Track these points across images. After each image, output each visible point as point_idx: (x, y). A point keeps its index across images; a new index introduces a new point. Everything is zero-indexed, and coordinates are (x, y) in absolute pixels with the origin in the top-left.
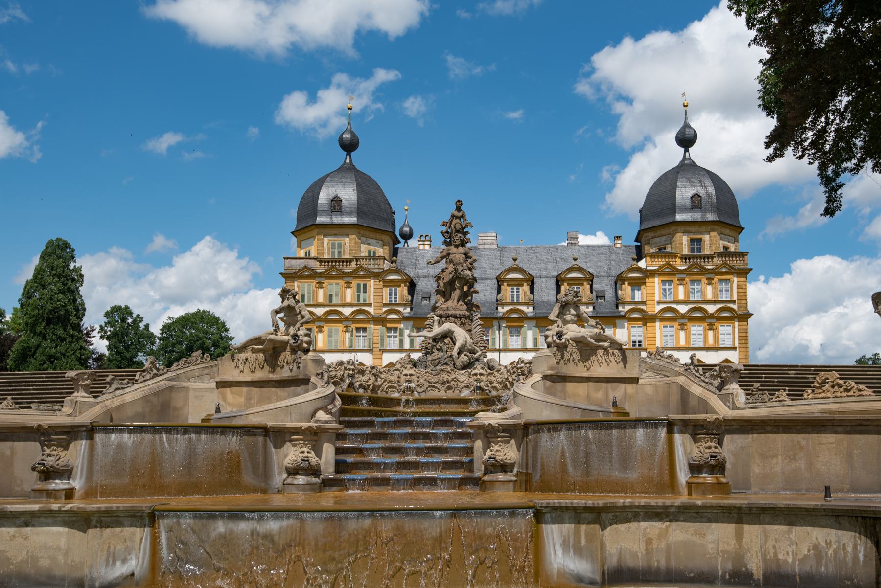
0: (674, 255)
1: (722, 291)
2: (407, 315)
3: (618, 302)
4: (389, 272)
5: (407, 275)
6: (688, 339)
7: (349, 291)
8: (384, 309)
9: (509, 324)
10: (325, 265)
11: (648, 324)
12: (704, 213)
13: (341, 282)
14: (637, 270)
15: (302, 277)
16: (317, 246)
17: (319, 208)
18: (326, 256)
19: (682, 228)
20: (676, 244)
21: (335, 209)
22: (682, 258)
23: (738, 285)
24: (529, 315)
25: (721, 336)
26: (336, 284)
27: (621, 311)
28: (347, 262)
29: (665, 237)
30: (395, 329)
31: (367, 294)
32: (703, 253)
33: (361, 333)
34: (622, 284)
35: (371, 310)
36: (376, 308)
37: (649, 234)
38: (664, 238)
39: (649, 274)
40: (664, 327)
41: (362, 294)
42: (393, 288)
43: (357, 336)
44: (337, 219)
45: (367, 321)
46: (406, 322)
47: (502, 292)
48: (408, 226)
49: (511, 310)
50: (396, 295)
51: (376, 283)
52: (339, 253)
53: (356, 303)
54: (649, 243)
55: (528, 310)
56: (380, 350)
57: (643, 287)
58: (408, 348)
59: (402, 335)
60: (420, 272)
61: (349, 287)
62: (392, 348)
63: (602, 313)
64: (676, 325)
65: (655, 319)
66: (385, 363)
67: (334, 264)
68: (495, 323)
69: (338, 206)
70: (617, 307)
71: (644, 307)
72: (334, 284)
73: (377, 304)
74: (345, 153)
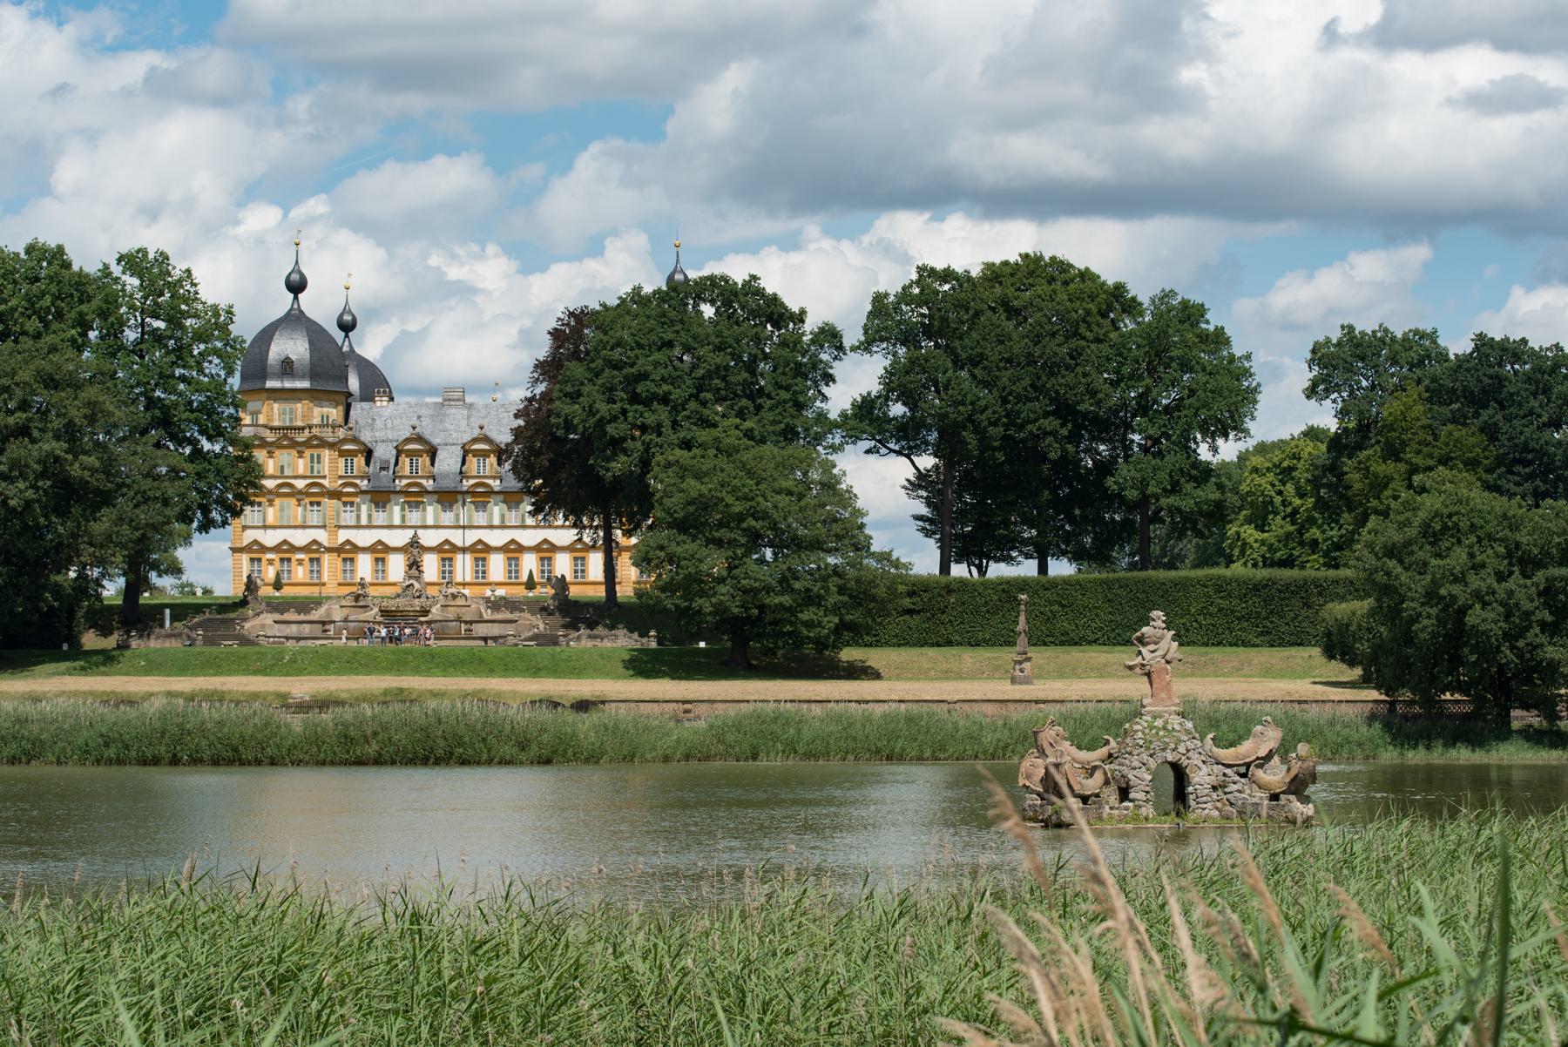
2: (364, 488)
4: (344, 441)
7: (301, 461)
8: (340, 482)
13: (294, 452)
18: (276, 423)
24: (496, 489)
33: (315, 508)
35: (325, 482)
41: (316, 465)
45: (321, 495)
46: (363, 496)
48: (350, 312)
52: (291, 419)
59: (359, 510)
60: (378, 434)
61: (301, 457)
62: (349, 523)
66: (340, 541)
68: (460, 497)
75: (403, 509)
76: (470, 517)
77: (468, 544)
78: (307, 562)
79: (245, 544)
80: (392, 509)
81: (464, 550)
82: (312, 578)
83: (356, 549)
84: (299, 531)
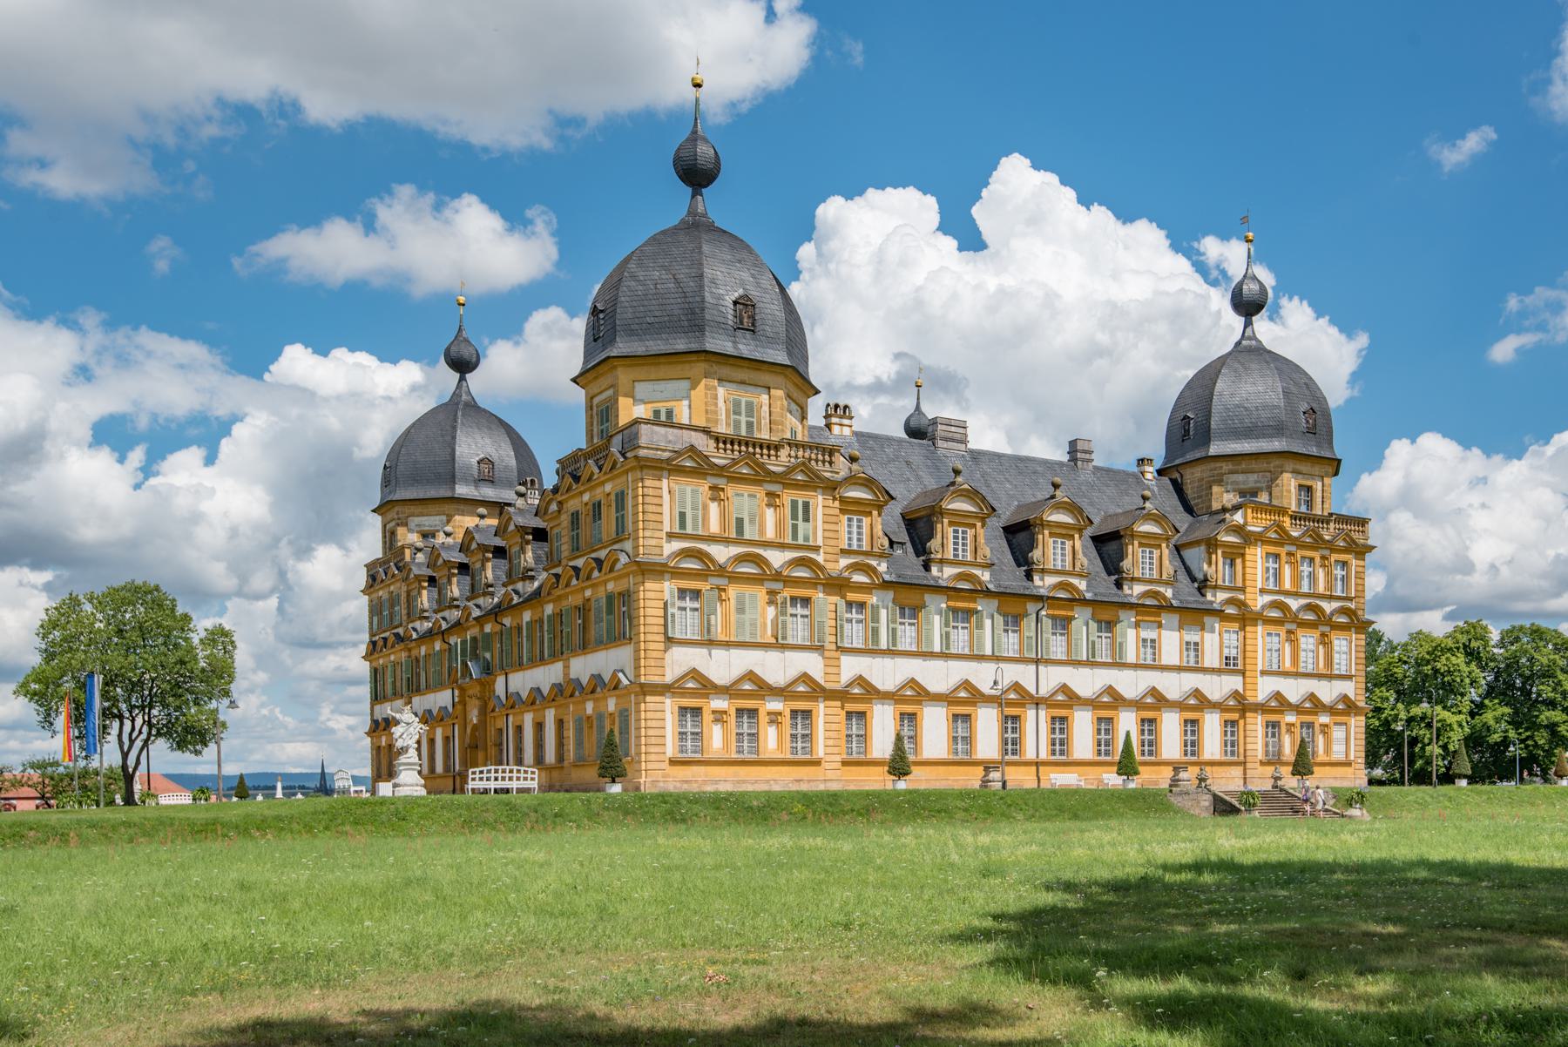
0: (1282, 511)
1: (1336, 579)
2: (887, 577)
3: (1203, 585)
4: (851, 480)
5: (887, 492)
6: (1295, 659)
7: (770, 514)
8: (844, 562)
9: (1051, 612)
10: (725, 450)
11: (1248, 629)
12: (1319, 445)
13: (760, 492)
14: (1234, 531)
15: (680, 471)
16: (706, 403)
17: (708, 317)
18: (722, 429)
19: (1289, 465)
20: (1282, 491)
21: (742, 323)
22: (1291, 516)
23: (1356, 572)
25: (1336, 656)
26: (749, 496)
27: (1212, 603)
28: (769, 448)
29: (1255, 476)
30: (861, 606)
31: (810, 525)
32: (1314, 512)
33: (799, 610)
34: (1210, 554)
35: (820, 558)
36: (828, 557)
37: (1224, 464)
38: (1253, 478)
39: (1249, 539)
40: (1269, 634)
41: (800, 523)
42: (855, 518)
43: (791, 615)
44: (746, 348)
45: (812, 583)
47: (1040, 546)
49: (1060, 583)
50: (859, 533)
51: (827, 503)
52: (750, 425)
53: (789, 540)
54: (1222, 481)
55: (1082, 585)
56: (838, 648)
57: (1239, 561)
58: (885, 648)
59: (876, 619)
62: (855, 645)
63: (1187, 602)
64: (1283, 635)
65: (1257, 619)
66: (846, 675)
67: (751, 450)
68: (1032, 607)
69: (749, 317)
70: (1203, 595)
71: (1242, 597)
72: (746, 494)
73: (829, 550)
74: (689, 190)
75: (947, 625)
76: (1048, 641)
77: (1044, 691)
78: (787, 720)
79: (668, 679)
80: (929, 622)
81: (1038, 703)
82: (794, 750)
83: (871, 693)
84: (773, 656)
